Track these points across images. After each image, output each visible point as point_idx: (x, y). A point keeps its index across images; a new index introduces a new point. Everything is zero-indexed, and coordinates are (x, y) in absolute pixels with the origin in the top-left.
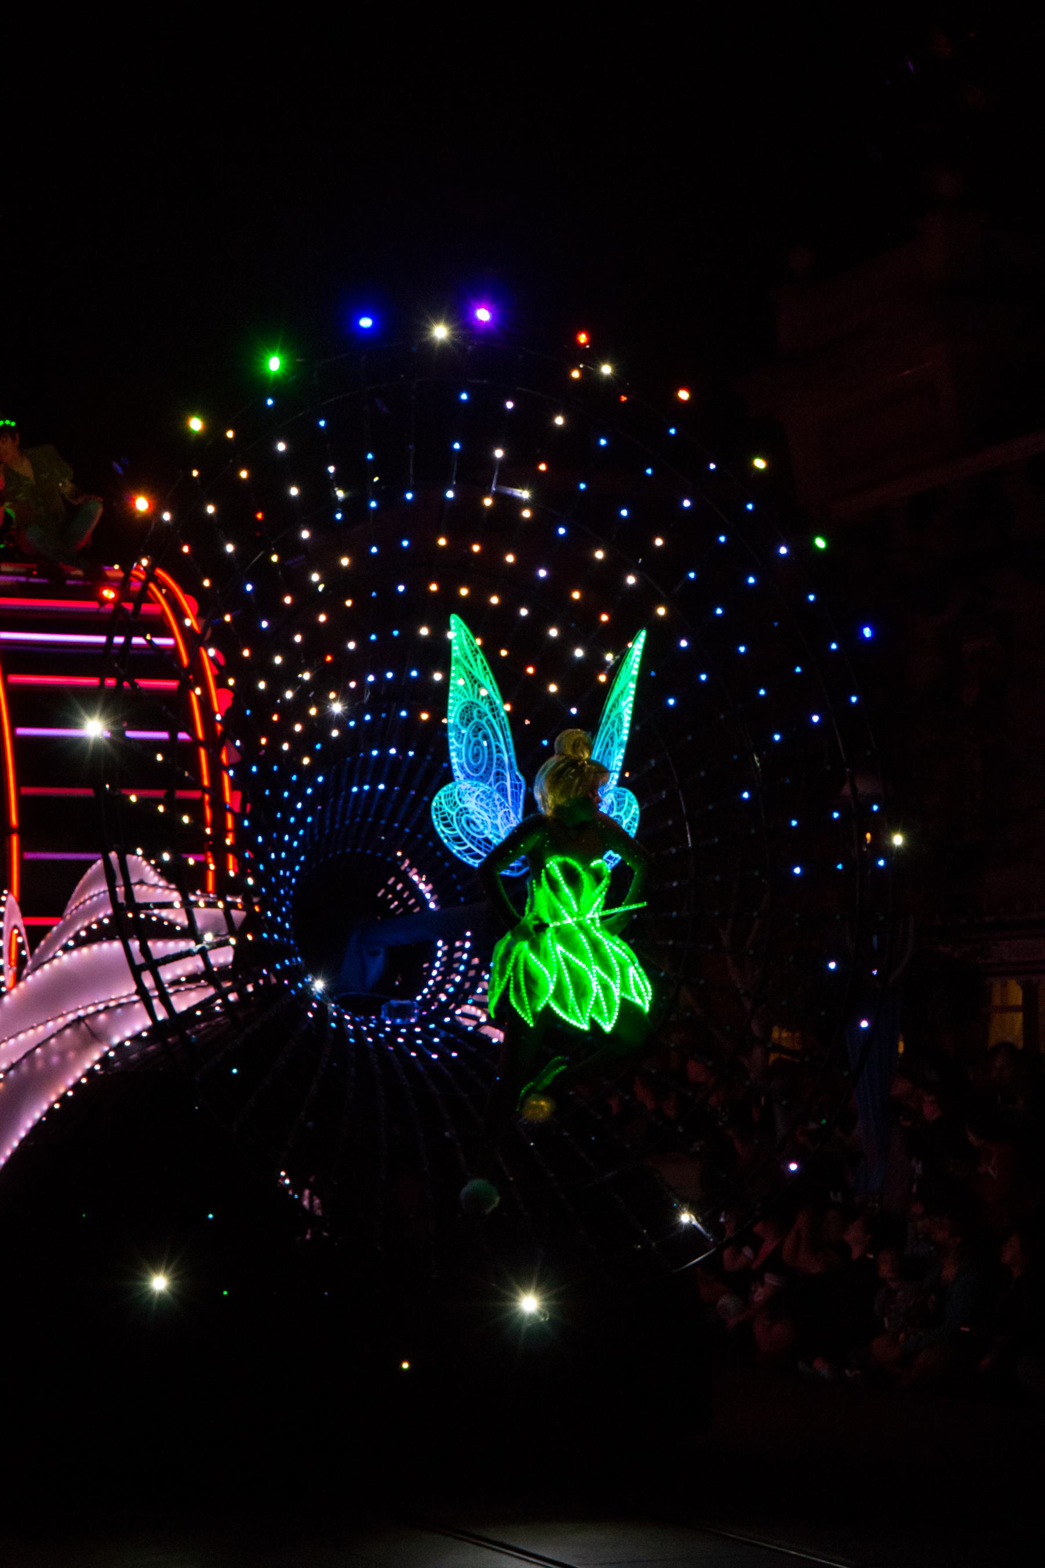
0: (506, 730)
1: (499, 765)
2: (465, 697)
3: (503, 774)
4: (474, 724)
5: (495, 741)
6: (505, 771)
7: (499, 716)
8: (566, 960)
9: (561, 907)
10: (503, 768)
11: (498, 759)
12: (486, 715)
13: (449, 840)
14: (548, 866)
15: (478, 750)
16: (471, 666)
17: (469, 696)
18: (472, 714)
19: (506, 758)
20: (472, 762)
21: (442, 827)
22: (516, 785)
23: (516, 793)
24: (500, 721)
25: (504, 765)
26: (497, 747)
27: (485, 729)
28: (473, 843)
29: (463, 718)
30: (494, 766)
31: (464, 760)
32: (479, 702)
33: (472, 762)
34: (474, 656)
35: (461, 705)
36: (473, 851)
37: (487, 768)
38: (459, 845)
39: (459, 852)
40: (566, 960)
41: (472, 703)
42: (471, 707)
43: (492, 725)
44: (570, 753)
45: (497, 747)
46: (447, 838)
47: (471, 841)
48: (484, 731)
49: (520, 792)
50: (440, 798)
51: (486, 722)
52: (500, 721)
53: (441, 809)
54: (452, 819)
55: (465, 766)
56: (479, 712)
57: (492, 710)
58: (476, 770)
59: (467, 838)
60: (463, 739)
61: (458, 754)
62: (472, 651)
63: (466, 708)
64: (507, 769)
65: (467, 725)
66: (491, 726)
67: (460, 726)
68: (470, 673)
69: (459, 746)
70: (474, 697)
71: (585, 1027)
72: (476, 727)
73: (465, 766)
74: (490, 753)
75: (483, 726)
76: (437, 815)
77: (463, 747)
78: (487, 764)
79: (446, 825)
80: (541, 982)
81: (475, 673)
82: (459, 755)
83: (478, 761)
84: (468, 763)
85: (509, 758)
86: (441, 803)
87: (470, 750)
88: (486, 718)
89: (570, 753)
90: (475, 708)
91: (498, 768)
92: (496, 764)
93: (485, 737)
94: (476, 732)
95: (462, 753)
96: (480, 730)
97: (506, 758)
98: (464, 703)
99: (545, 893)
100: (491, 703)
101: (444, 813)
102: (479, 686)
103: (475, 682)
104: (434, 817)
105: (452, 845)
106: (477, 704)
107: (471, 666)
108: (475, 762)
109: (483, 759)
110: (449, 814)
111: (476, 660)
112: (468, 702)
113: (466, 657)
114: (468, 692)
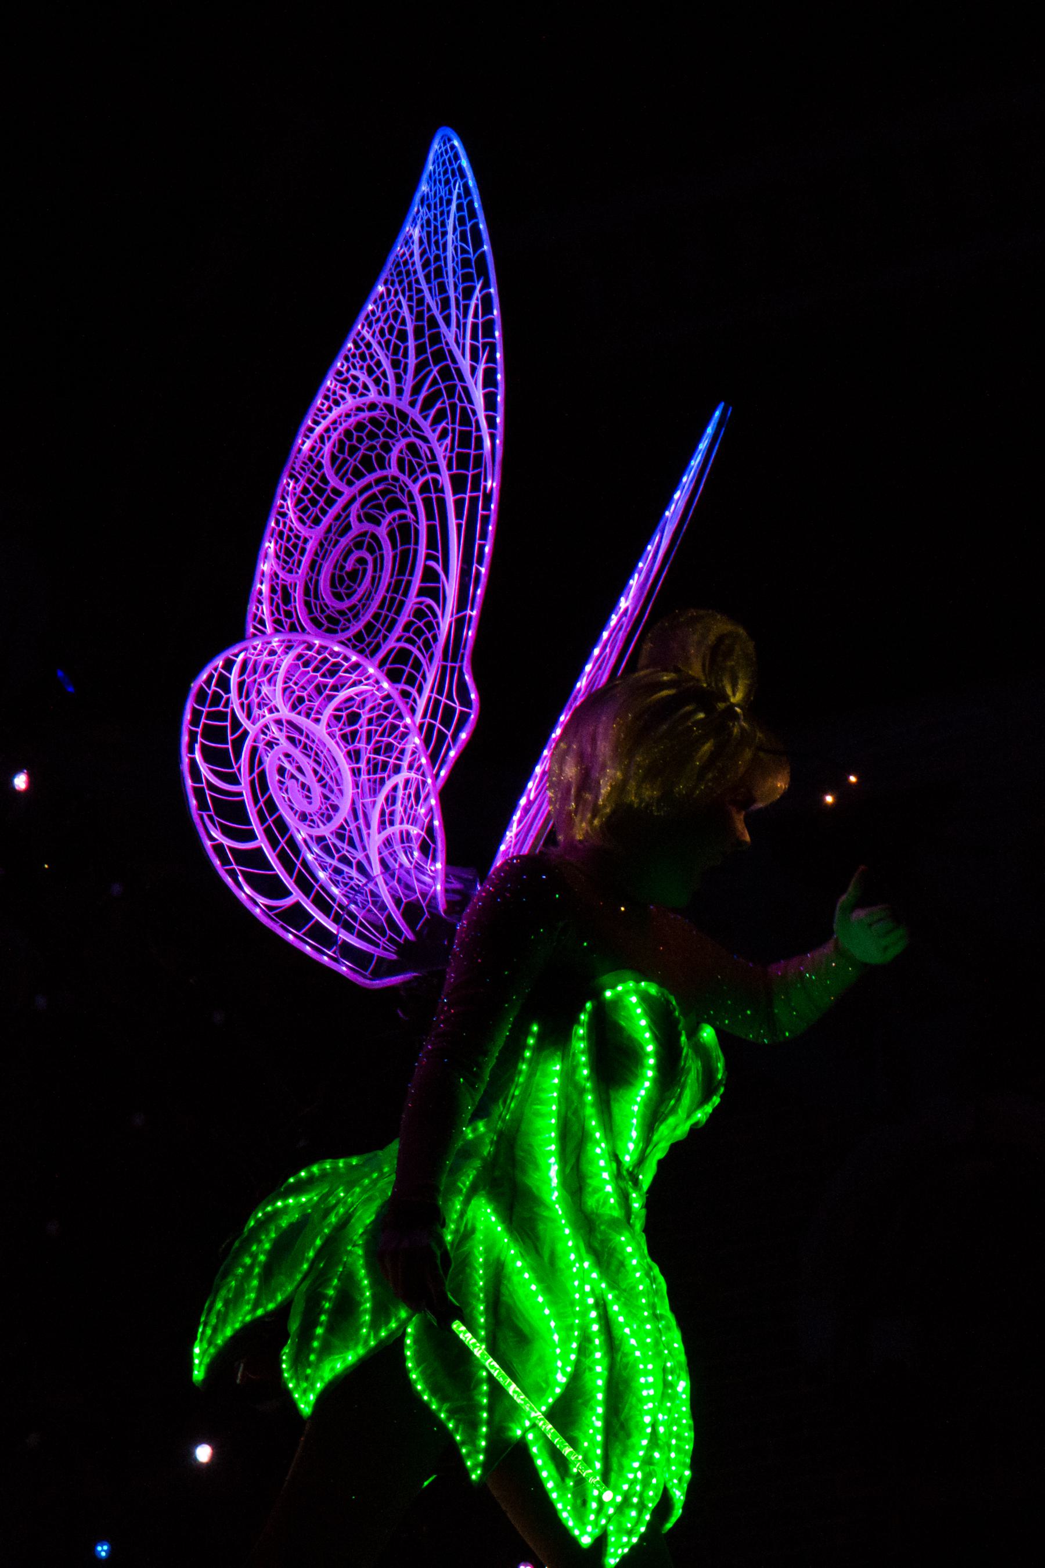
0: (484, 536)
1: (419, 632)
2: (386, 389)
3: (417, 665)
4: (378, 482)
5: (429, 557)
6: (431, 659)
7: (476, 487)
8: (601, 1305)
9: (598, 1135)
10: (428, 645)
11: (419, 613)
12: (435, 469)
13: (202, 805)
14: (608, 994)
15: (362, 561)
16: (445, 304)
17: (400, 392)
18: (387, 448)
19: (445, 624)
20: (326, 597)
21: (198, 756)
22: (449, 711)
23: (442, 737)
24: (474, 501)
25: (435, 639)
26: (430, 575)
27: (414, 509)
28: (274, 843)
29: (353, 450)
30: (399, 628)
31: (298, 579)
32: (425, 425)
33: (326, 597)
34: (467, 278)
35: (359, 409)
36: (268, 866)
37: (369, 627)
38: (226, 832)
39: (219, 849)
40: (601, 1305)
41: (403, 416)
42: (392, 424)
43: (442, 502)
44: (696, 670)
45: (430, 575)
46: (199, 793)
47: (268, 833)
48: (408, 513)
49: (455, 736)
50: (229, 665)
51: (425, 489)
52: (474, 501)
53: (216, 699)
54: (238, 744)
55: (297, 594)
56: (412, 448)
57: (463, 461)
58: (330, 619)
59: (262, 819)
60: (324, 512)
61: (288, 553)
62: (466, 263)
63: (373, 421)
64: (438, 650)
65: (358, 474)
66: (436, 509)
67: (328, 471)
68: (433, 322)
69: (304, 532)
70: (412, 404)
71: (586, 1541)
72: (384, 493)
73: (297, 594)
74: (399, 587)
75: (411, 497)
76: (196, 715)
77: (312, 536)
78: (376, 616)
79: (209, 755)
80: (538, 1348)
81: (449, 335)
82: (287, 556)
83: (349, 596)
84: (311, 591)
85: (460, 624)
86: (224, 683)
87: (334, 554)
88: (429, 476)
89: (696, 670)
90: (405, 435)
91: (410, 641)
92: (407, 627)
93: (404, 533)
94: (379, 507)
95: (303, 551)
96: (395, 504)
97: (445, 624)
98: (373, 406)
99: (569, 1076)
100: (465, 439)
101: (222, 716)
102: (445, 374)
103: (440, 356)
104: (188, 716)
105: (209, 825)
106: (415, 425)
107: (445, 304)
108: (338, 597)
109: (369, 596)
110: (236, 724)
111: (468, 293)
112: (389, 407)
113: (439, 272)
114: (398, 378)
